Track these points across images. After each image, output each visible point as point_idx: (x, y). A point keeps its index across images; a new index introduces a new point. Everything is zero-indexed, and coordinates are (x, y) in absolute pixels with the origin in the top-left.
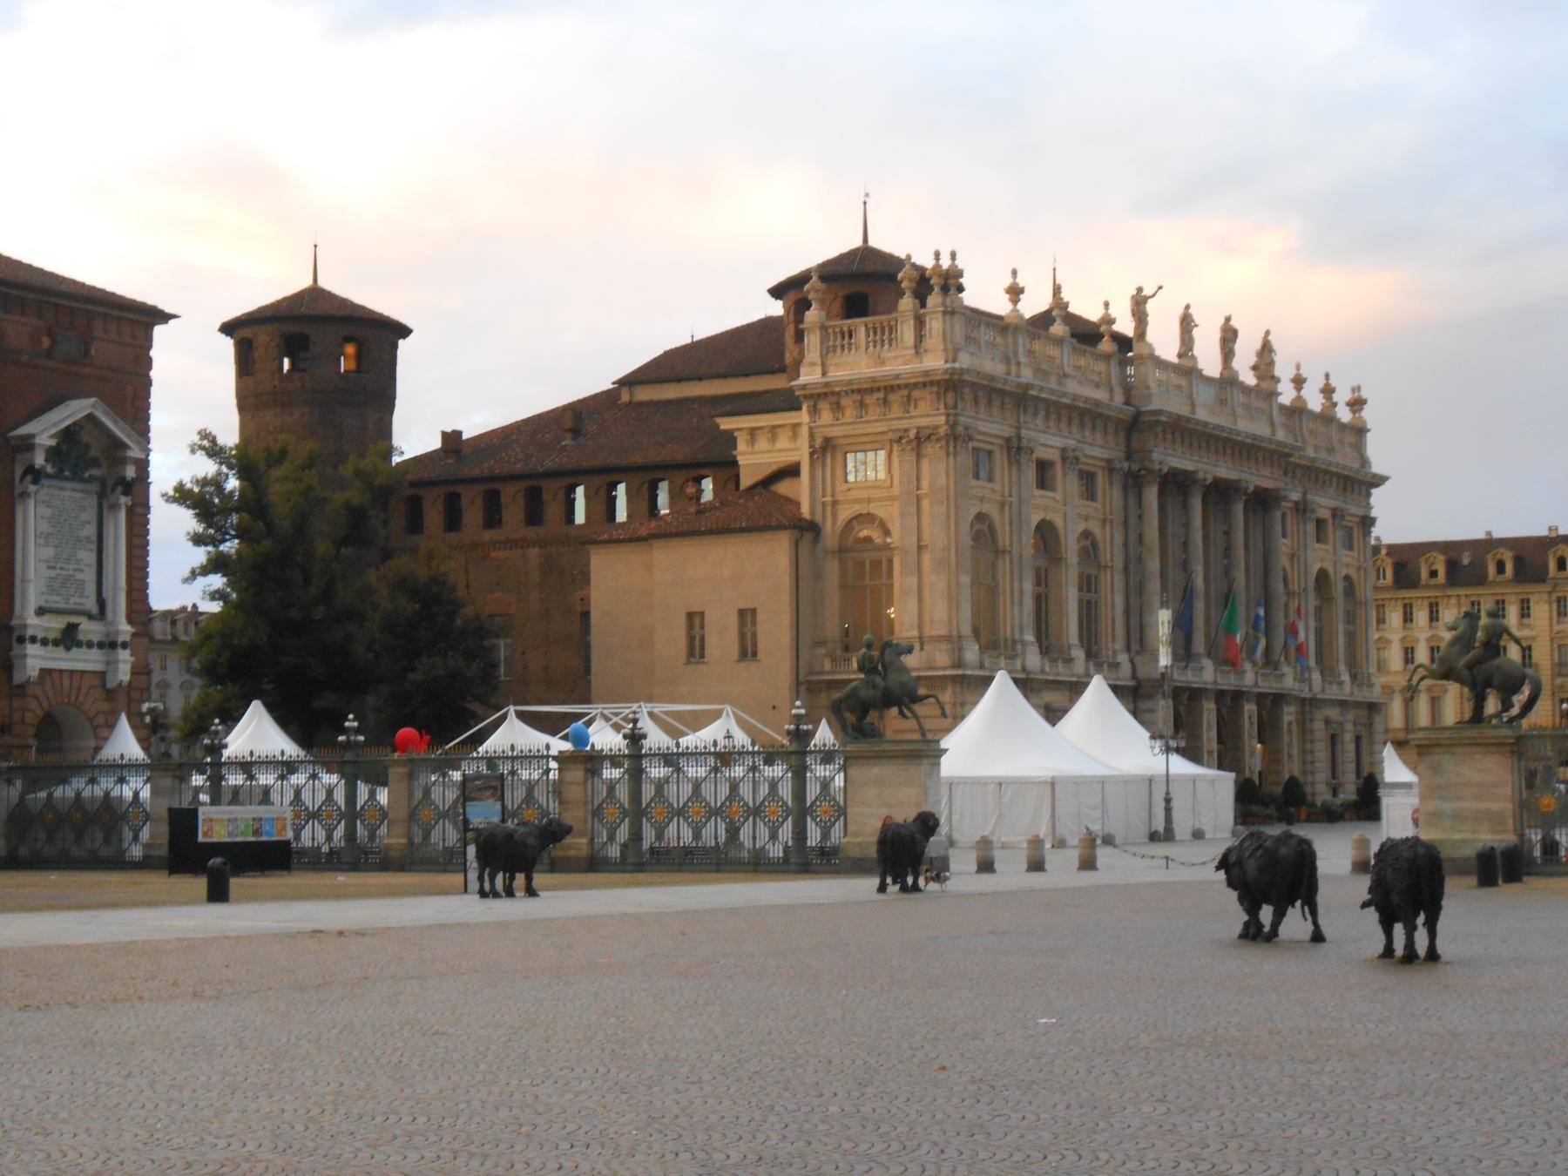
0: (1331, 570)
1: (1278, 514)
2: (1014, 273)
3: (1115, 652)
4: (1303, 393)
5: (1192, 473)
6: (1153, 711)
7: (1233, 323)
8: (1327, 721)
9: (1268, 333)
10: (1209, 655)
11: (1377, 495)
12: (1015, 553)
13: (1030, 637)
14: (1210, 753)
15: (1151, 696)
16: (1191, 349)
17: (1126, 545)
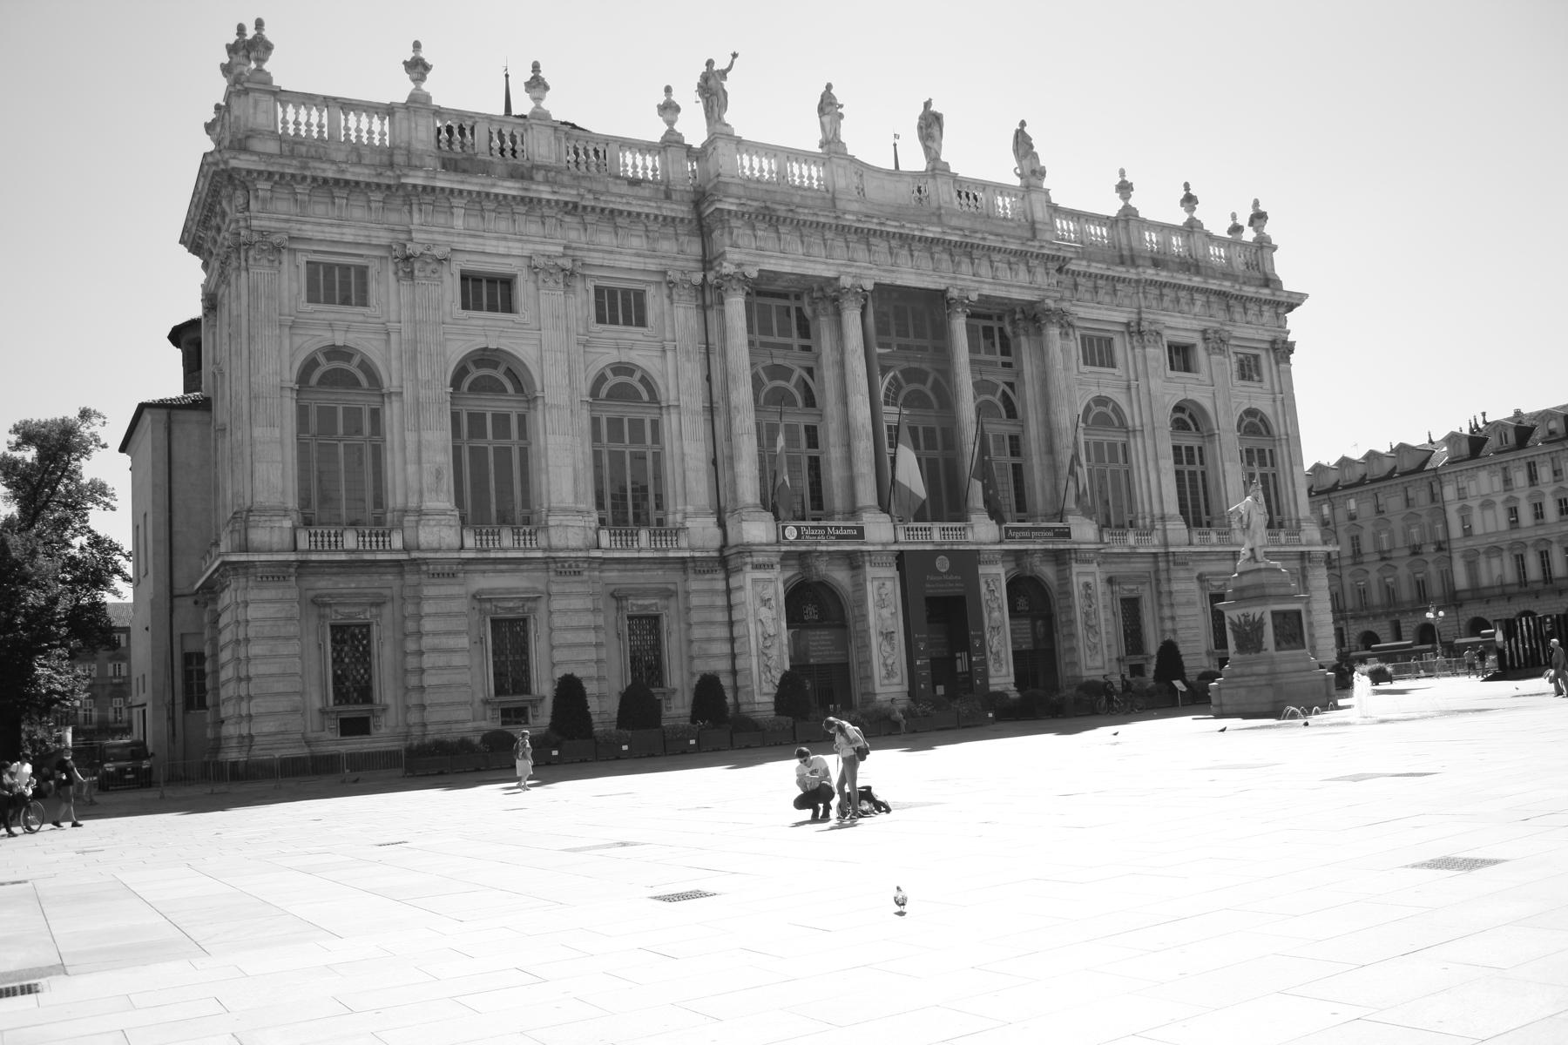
0: (1207, 405)
1: (1053, 332)
3: (685, 517)
4: (1131, 202)
5: (837, 279)
6: (741, 588)
7: (933, 108)
8: (1201, 578)
9: (1023, 124)
10: (884, 506)
11: (1293, 320)
12: (408, 395)
13: (442, 501)
14: (888, 636)
15: (739, 570)
16: (836, 134)
17: (709, 378)
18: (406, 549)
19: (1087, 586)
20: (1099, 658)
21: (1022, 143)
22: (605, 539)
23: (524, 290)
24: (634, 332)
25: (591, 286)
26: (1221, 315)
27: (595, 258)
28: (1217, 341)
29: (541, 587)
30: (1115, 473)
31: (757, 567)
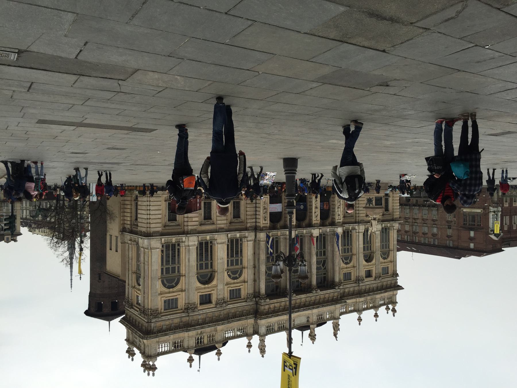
0: (199, 285)
2: (376, 320)
8: (213, 224)
18: (382, 224)
19: (265, 220)
20: (264, 200)
21: (262, 350)
22: (357, 227)
23: (364, 275)
24: (345, 271)
25: (353, 279)
26: (184, 319)
27: (354, 285)
28: (189, 308)
29: (365, 218)
30: (232, 256)
31: (340, 222)
